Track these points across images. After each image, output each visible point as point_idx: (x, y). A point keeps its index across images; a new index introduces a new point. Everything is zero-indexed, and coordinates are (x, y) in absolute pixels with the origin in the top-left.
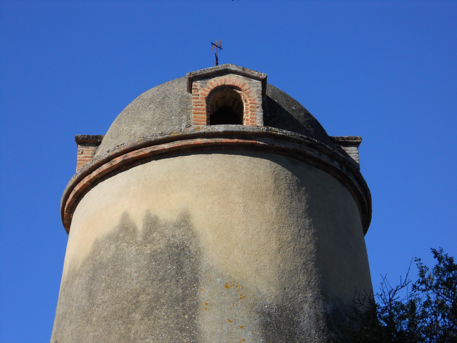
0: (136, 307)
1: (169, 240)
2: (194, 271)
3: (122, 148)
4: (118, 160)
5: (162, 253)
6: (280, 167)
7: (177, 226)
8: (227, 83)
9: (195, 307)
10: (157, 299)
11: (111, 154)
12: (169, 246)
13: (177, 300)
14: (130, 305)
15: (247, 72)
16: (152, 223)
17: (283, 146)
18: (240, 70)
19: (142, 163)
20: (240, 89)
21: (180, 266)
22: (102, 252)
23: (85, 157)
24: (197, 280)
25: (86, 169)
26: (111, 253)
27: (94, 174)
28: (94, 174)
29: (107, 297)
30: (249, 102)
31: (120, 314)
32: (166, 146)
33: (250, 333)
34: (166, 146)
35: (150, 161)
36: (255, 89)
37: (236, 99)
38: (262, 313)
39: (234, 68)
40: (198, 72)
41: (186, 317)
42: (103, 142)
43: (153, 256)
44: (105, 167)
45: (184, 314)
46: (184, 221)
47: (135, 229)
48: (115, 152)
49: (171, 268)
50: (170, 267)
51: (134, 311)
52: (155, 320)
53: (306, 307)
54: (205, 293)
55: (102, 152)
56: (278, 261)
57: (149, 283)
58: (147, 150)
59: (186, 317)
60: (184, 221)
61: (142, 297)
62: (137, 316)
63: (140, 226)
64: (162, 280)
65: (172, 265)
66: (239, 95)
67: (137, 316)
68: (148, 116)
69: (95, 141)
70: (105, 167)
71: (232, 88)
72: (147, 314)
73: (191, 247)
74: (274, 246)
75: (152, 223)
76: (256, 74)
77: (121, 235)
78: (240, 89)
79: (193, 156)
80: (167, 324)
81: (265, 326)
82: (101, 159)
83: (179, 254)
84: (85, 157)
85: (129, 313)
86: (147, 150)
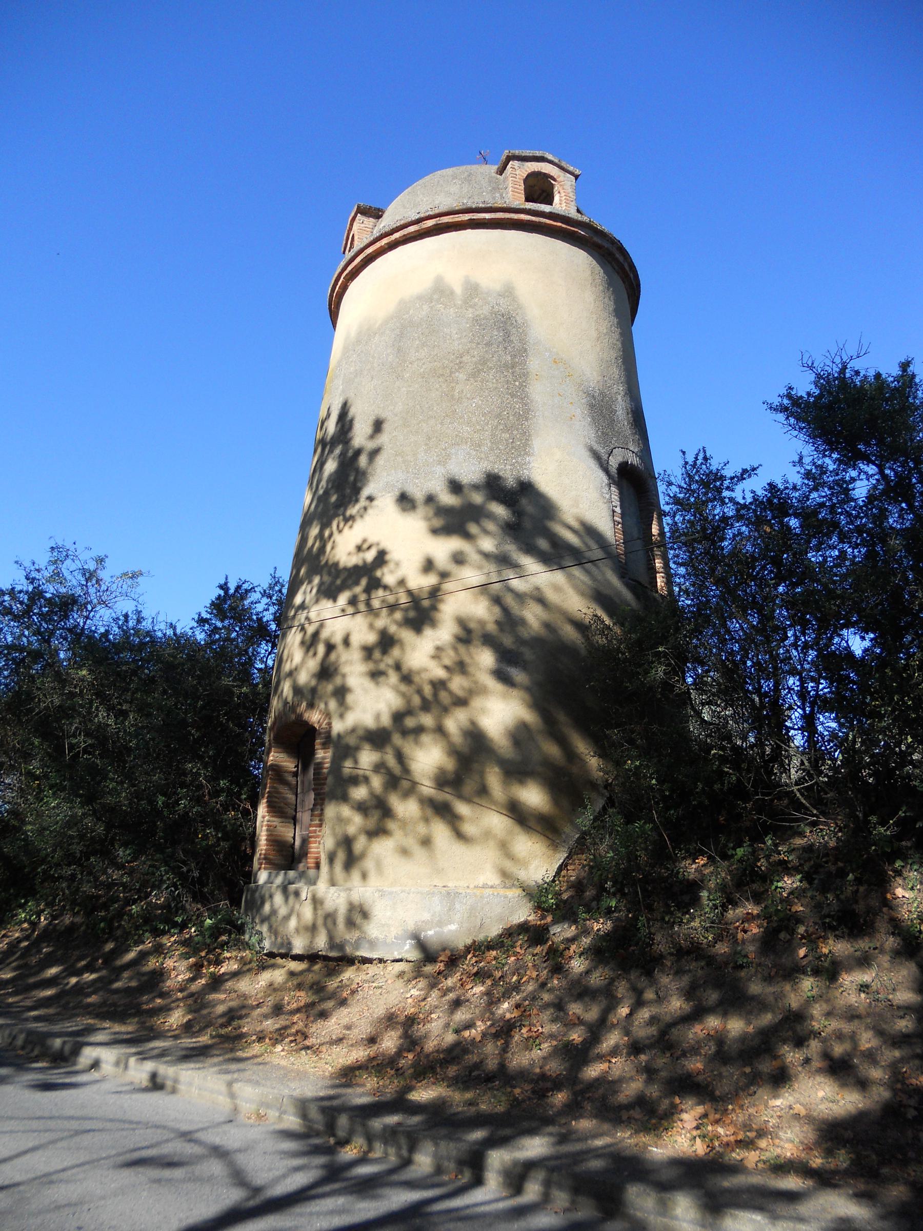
0: (460, 368)
1: (493, 307)
2: (522, 341)
3: (437, 211)
4: (430, 223)
5: (485, 318)
6: (594, 262)
7: (501, 295)
8: (543, 171)
9: (525, 375)
10: (483, 362)
11: (422, 215)
12: (494, 313)
13: (506, 366)
14: (452, 365)
15: (563, 164)
16: (472, 290)
17: (600, 242)
18: (556, 161)
19: (456, 230)
20: (555, 180)
21: (507, 334)
22: (411, 312)
23: (364, 230)
24: (526, 350)
25: (387, 229)
26: (424, 313)
27: (397, 235)
28: (397, 235)
29: (423, 354)
30: (563, 194)
31: (441, 372)
32: (487, 216)
33: (579, 411)
34: (487, 216)
35: (465, 229)
36: (569, 183)
37: (543, 191)
38: (590, 395)
39: (550, 157)
40: (517, 152)
41: (517, 383)
42: (384, 216)
43: (476, 320)
44: (412, 229)
45: (515, 381)
46: (508, 292)
47: (452, 292)
48: (427, 214)
49: (498, 335)
50: (496, 333)
51: (457, 371)
52: (482, 383)
53: (619, 398)
54: (534, 364)
56: (598, 350)
57: (474, 345)
58: (466, 217)
59: (517, 383)
60: (508, 292)
61: (466, 358)
62: (461, 376)
63: (458, 290)
64: (488, 344)
65: (499, 331)
66: (552, 186)
67: (461, 376)
68: (454, 189)
69: (377, 214)
70: (412, 229)
71: (546, 177)
72: (474, 375)
73: (518, 318)
74: (594, 334)
75: (472, 290)
76: (571, 168)
77: (435, 297)
78: (555, 180)
79: (513, 231)
80: (496, 388)
81: (591, 406)
82: (410, 220)
83: (505, 323)
84: (364, 230)
85: (451, 373)
86: (466, 217)
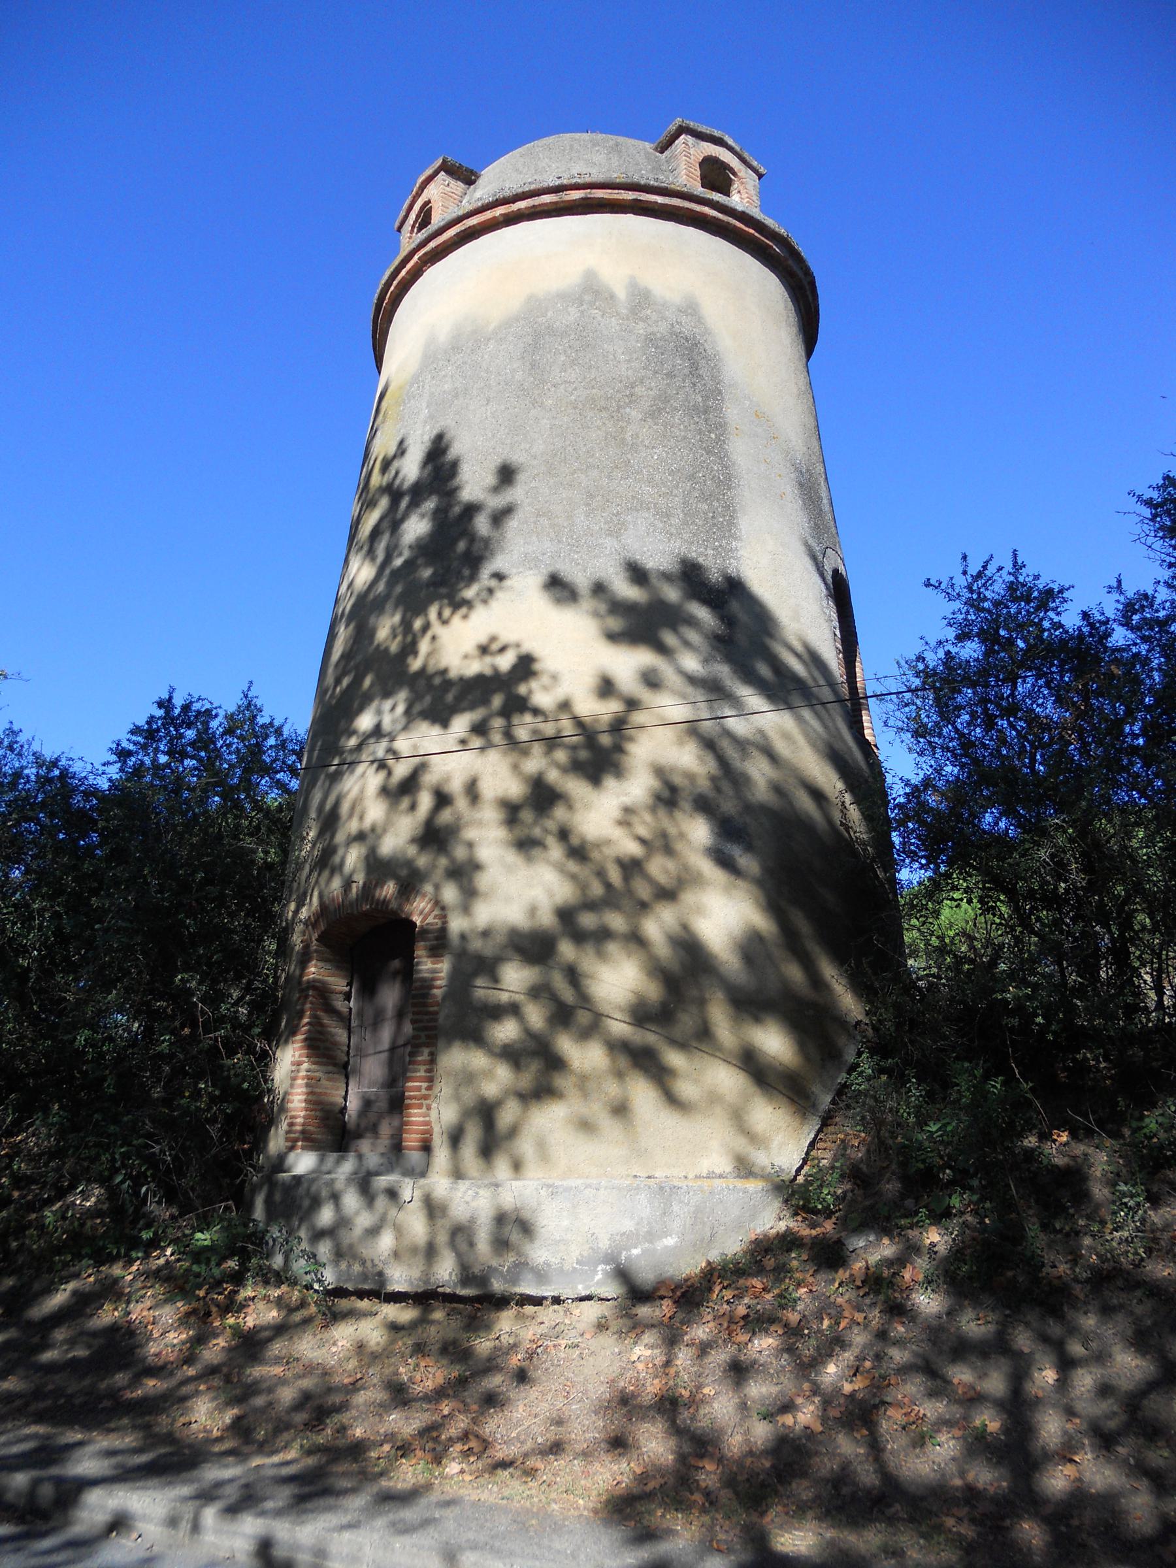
3: (588, 179)
4: (576, 195)
5: (663, 339)
11: (565, 182)
13: (696, 408)
15: (746, 155)
18: (737, 148)
20: (734, 174)
21: (695, 366)
23: (445, 198)
24: (720, 393)
26: (571, 319)
31: (603, 403)
39: (730, 142)
40: (692, 124)
42: (480, 182)
43: (650, 339)
44: (547, 199)
45: (709, 432)
46: (691, 308)
47: (612, 296)
48: (574, 181)
51: (629, 405)
52: (665, 427)
54: (732, 413)
55: (483, 191)
57: (650, 374)
58: (630, 196)
59: (713, 436)
60: (691, 308)
61: (639, 390)
62: (634, 414)
63: (621, 294)
64: (671, 375)
67: (634, 414)
69: (468, 178)
70: (547, 199)
71: (725, 167)
72: (653, 414)
75: (641, 299)
76: (755, 163)
80: (685, 438)
82: (545, 185)
85: (619, 407)
86: (630, 196)
